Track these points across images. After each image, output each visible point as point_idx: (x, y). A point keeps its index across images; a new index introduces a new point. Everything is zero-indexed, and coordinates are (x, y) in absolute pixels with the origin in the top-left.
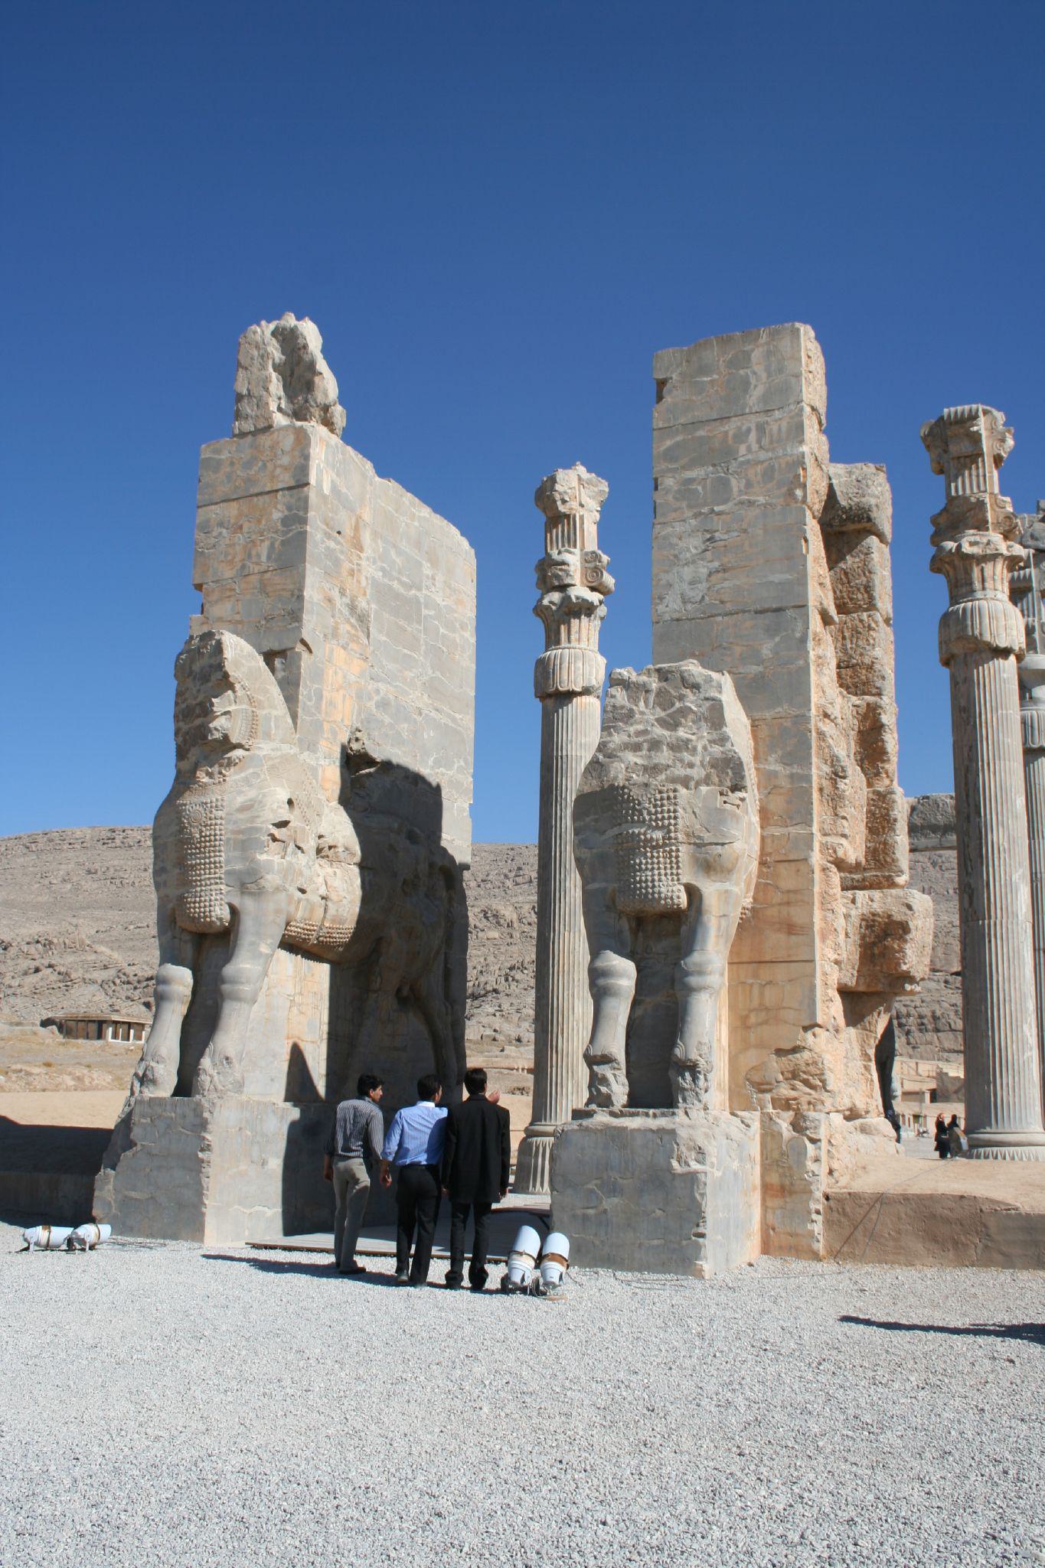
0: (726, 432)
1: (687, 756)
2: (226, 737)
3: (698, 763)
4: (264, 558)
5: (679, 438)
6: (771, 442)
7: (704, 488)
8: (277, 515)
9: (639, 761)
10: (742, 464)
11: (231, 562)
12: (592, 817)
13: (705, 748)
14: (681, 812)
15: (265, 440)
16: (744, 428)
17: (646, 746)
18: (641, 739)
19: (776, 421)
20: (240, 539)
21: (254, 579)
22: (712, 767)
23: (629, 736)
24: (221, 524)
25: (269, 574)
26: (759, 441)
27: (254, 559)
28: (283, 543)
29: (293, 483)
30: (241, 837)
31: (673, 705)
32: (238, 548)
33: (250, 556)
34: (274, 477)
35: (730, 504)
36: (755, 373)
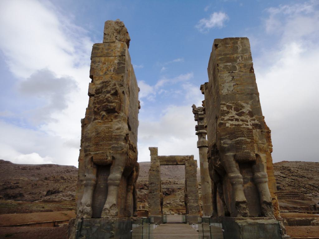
0: (234, 57)
1: (245, 123)
2: (114, 108)
3: (249, 125)
4: (112, 71)
5: (223, 56)
6: (245, 59)
7: (230, 67)
8: (116, 61)
9: (234, 123)
10: (238, 63)
11: (102, 71)
12: (228, 136)
13: (250, 121)
14: (254, 135)
15: (113, 45)
16: (238, 56)
17: (234, 120)
18: (233, 118)
19: (245, 55)
20: (105, 67)
21: (109, 76)
22: (253, 126)
23: (229, 117)
24: (99, 62)
25: (114, 75)
26: (242, 59)
27: (109, 71)
28: (118, 68)
29: (120, 55)
30: (118, 137)
31: (239, 111)
32: (104, 68)
33: (108, 70)
34: (115, 53)
35: (237, 71)
36: (239, 46)
